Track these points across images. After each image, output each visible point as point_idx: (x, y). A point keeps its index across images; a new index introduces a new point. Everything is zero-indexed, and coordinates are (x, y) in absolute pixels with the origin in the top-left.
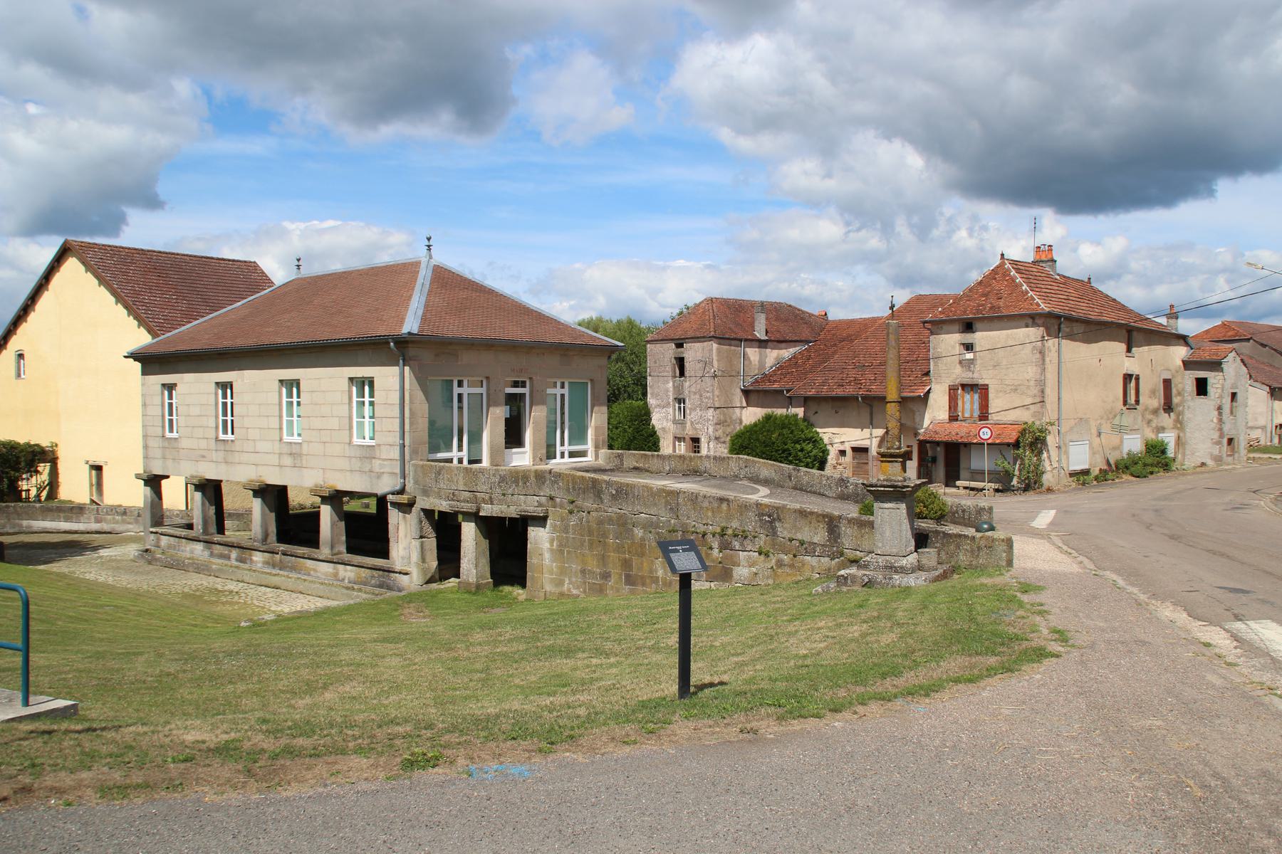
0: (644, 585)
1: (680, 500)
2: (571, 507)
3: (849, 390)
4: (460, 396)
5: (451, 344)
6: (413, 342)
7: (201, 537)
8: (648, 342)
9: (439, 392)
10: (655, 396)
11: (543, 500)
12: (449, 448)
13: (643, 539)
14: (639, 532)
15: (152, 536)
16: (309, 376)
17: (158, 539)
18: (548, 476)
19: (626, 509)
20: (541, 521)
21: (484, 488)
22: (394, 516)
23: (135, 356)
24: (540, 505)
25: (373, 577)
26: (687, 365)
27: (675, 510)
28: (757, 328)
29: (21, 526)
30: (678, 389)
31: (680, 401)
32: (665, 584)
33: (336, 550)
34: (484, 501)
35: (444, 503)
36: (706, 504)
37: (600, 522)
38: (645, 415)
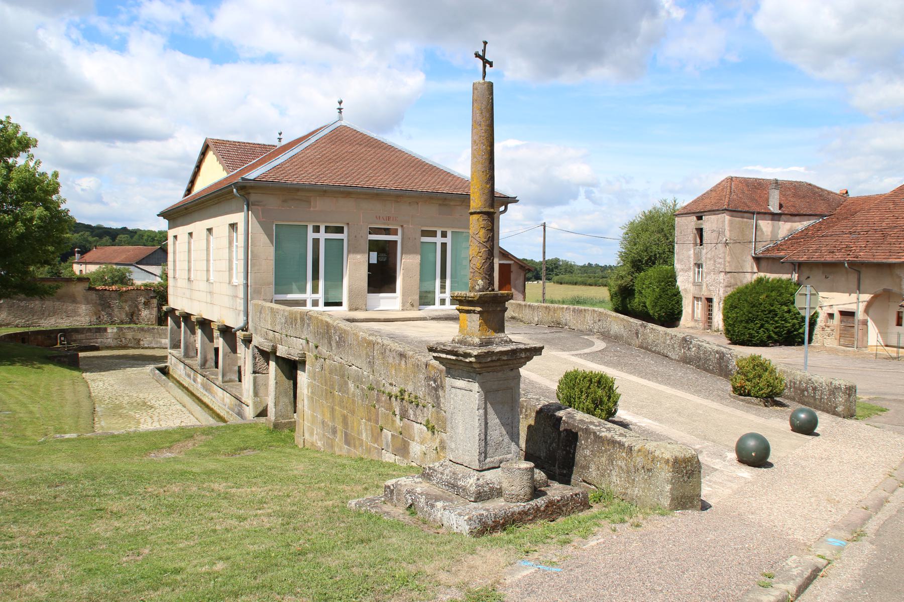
3: (838, 257)
4: (316, 242)
5: (298, 190)
6: (252, 187)
8: (676, 215)
9: (284, 238)
10: (680, 261)
12: (303, 291)
26: (704, 234)
28: (771, 203)
29: (161, 343)
30: (697, 255)
31: (699, 266)
33: (227, 378)
38: (671, 279)
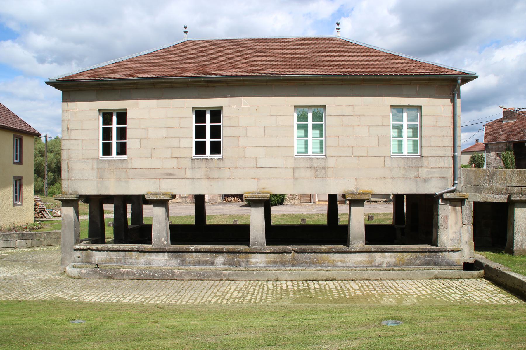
15: (78, 253)
17: (88, 256)
22: (445, 211)
23: (57, 84)
35: (497, 196)
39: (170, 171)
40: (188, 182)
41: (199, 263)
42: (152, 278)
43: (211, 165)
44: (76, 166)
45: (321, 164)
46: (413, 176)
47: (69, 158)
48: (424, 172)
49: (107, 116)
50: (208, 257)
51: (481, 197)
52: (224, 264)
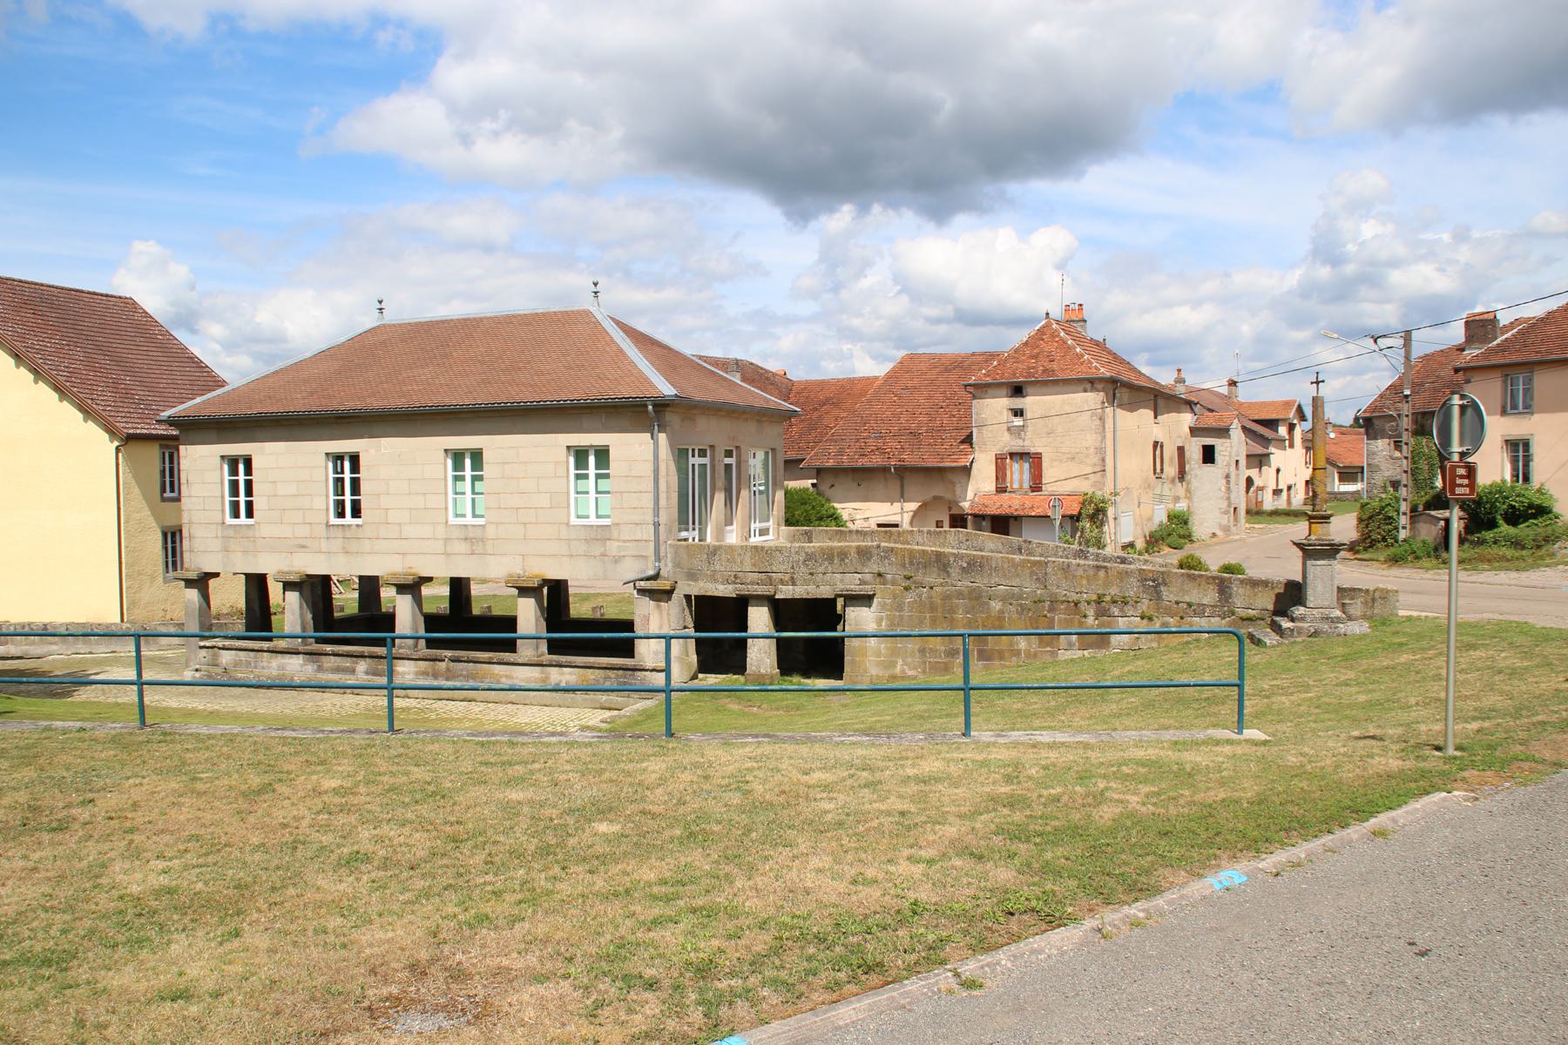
0: (1001, 659)
1: (1049, 570)
2: (908, 583)
3: (876, 460)
7: (301, 648)
11: (868, 577)
13: (1001, 612)
14: (996, 605)
15: (203, 652)
16: (496, 446)
17: (215, 656)
18: (875, 551)
19: (981, 582)
20: (865, 600)
21: (782, 568)
24: (863, 582)
25: (606, 678)
27: (1043, 581)
32: (1028, 655)
34: (782, 582)
35: (721, 587)
36: (1080, 572)
37: (946, 597)
39: (303, 542)
40: (323, 556)
41: (338, 670)
42: (269, 687)
43: (348, 534)
44: (198, 532)
45: (478, 533)
46: (597, 553)
47: (190, 523)
48: (613, 548)
49: (233, 463)
50: (347, 663)
51: (697, 589)
52: (367, 673)
